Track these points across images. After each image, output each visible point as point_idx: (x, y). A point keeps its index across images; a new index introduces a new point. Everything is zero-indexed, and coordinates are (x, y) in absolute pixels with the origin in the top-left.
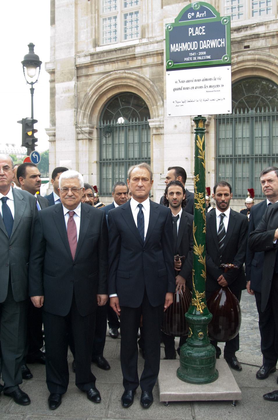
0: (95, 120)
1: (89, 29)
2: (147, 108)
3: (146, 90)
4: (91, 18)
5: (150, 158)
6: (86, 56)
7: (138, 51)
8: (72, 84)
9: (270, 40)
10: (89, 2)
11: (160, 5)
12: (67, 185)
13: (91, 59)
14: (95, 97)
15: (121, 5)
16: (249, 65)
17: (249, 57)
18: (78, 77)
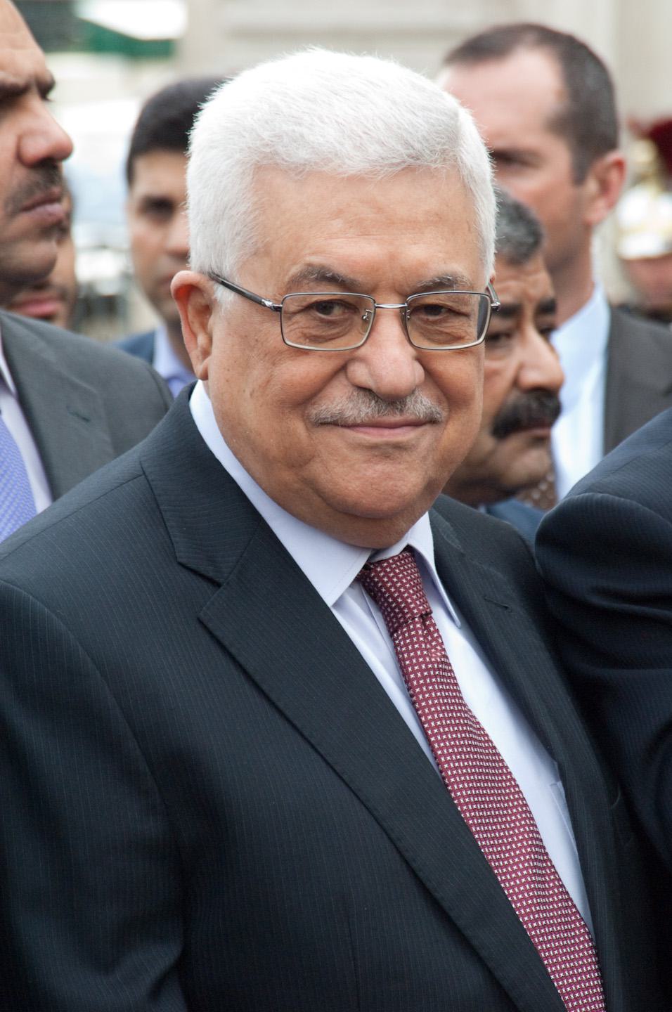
12: (350, 251)
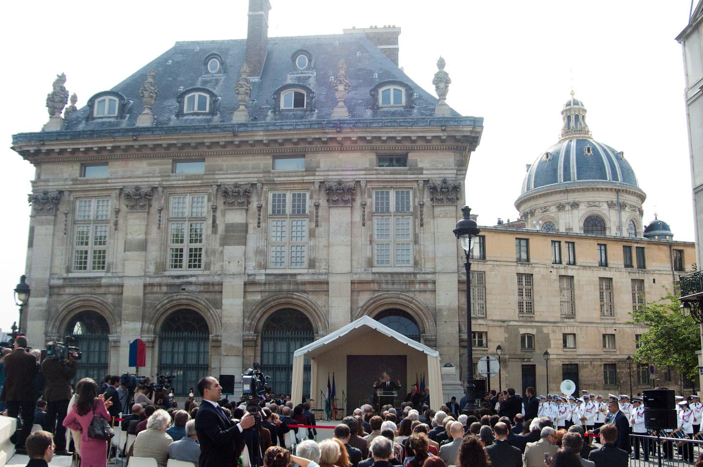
0: (62, 331)
1: (63, 257)
2: (107, 325)
3: (108, 312)
4: (66, 249)
5: (107, 364)
6: (59, 279)
7: (104, 281)
8: (45, 300)
9: (199, 287)
10: (65, 236)
11: (123, 249)
13: (64, 282)
14: (64, 313)
15: (92, 243)
16: (184, 302)
17: (185, 297)
18: (50, 295)
